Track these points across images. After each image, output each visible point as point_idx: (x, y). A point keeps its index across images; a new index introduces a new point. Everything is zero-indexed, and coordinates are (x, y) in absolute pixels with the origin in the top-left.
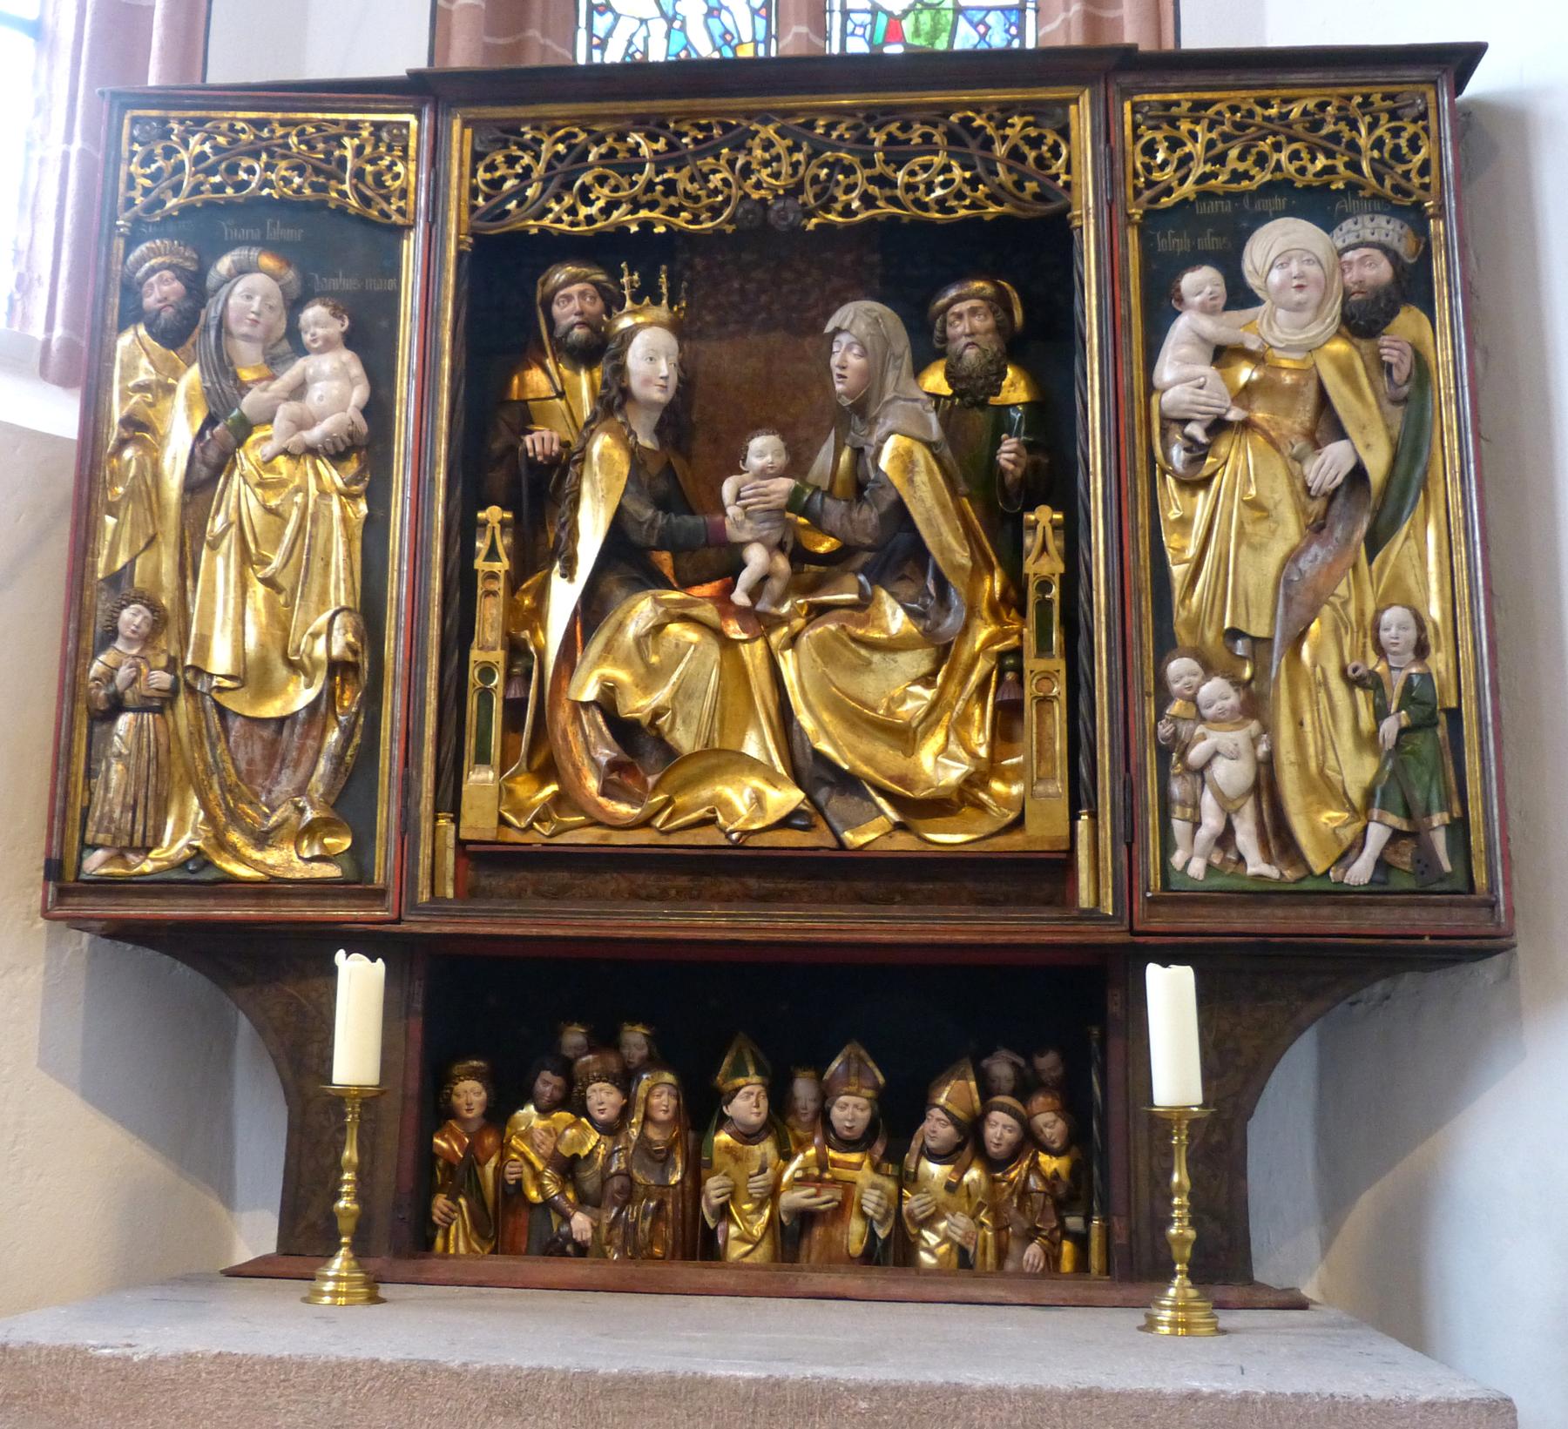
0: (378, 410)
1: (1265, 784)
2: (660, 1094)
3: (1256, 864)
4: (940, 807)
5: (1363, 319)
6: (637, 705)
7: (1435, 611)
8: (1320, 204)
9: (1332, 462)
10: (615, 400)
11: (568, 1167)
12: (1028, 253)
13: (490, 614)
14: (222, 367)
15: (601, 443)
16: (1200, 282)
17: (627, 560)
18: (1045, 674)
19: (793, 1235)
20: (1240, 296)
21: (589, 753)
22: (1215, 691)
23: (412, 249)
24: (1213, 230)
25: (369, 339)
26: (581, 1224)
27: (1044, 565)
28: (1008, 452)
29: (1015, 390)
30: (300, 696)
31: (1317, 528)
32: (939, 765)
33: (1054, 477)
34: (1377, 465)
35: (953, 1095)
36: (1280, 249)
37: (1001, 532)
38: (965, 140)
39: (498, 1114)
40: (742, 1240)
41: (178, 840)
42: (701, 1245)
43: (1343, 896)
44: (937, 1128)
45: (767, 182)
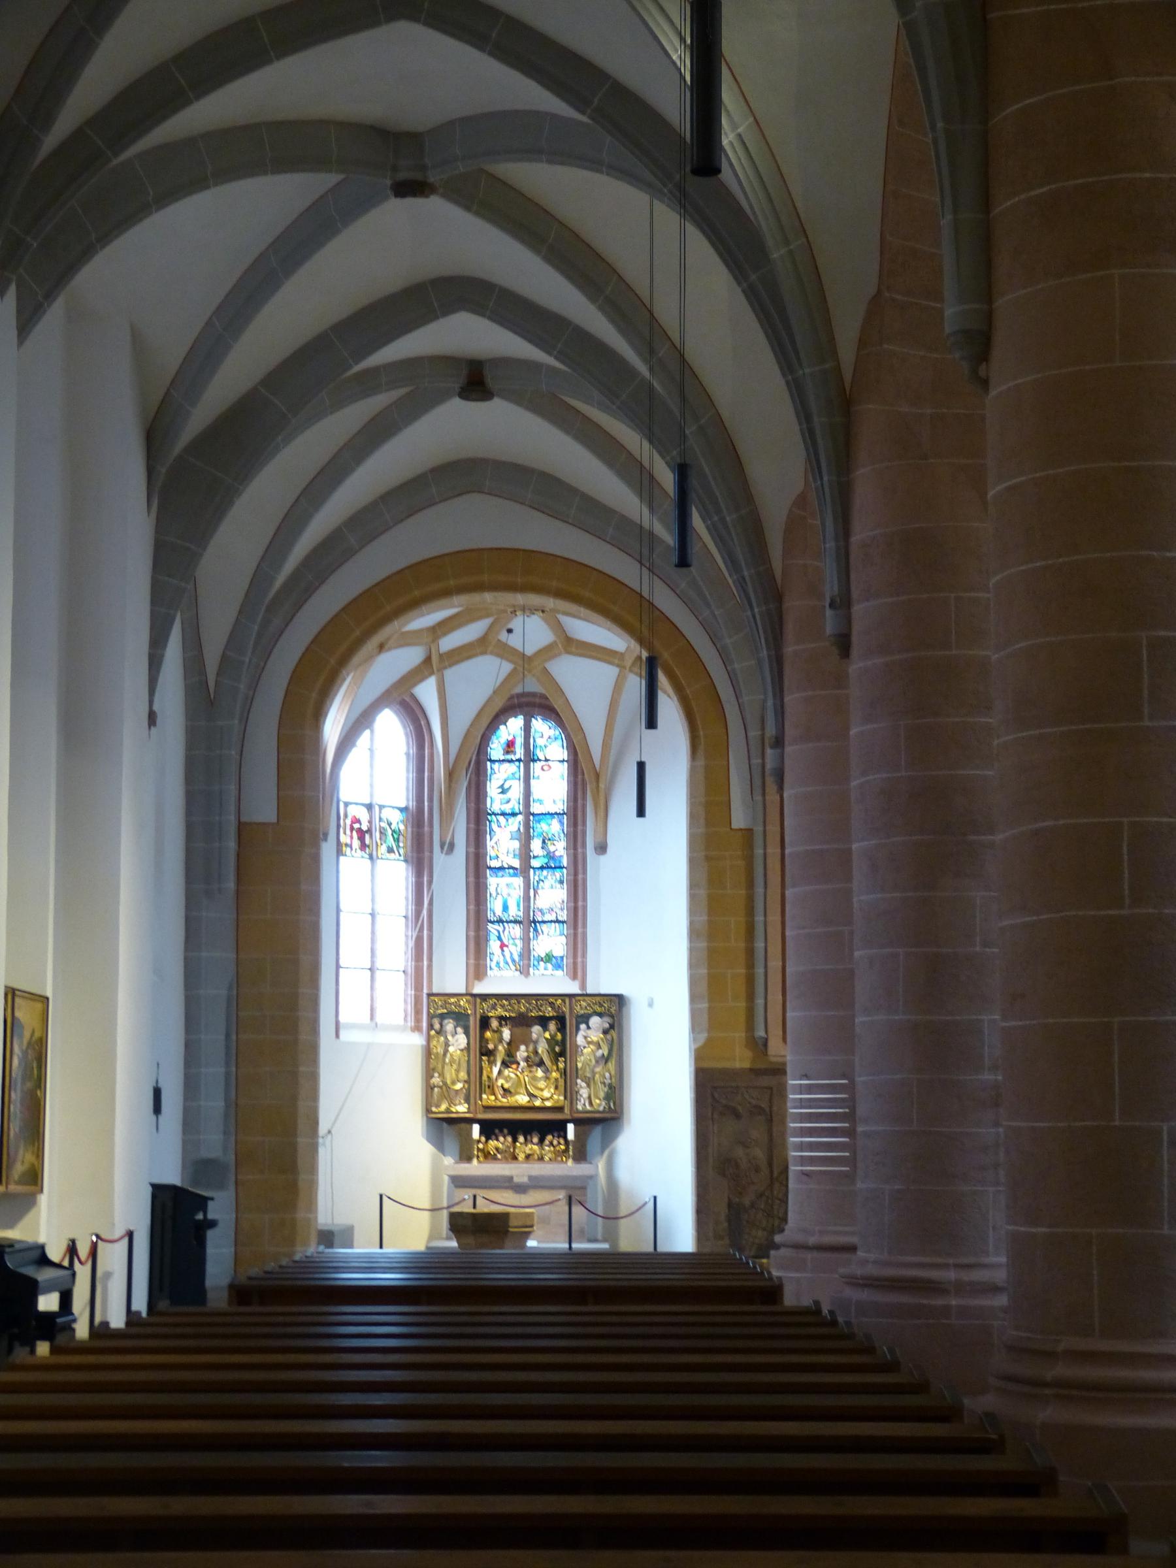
0: (468, 1044)
1: (589, 1098)
2: (509, 1139)
3: (588, 1108)
4: (547, 1099)
5: (605, 1032)
6: (506, 1086)
7: (613, 1073)
8: (600, 1015)
9: (600, 1053)
10: (501, 1040)
11: (497, 1149)
12: (561, 1020)
13: (485, 1073)
14: (446, 1038)
15: (500, 1048)
16: (583, 1026)
17: (505, 1064)
18: (561, 1082)
19: (528, 1157)
20: (589, 1028)
21: (499, 1092)
22: (584, 1084)
23: (472, 1019)
24: (585, 1019)
25: (467, 1033)
26: (499, 1156)
27: (561, 1065)
28: (557, 1049)
29: (559, 1036)
30: (459, 1086)
31: (597, 1062)
32: (546, 1094)
33: (562, 1054)
34: (606, 1054)
35: (549, 1137)
36: (595, 1021)
37: (555, 1061)
38: (552, 1004)
39: (487, 1141)
40: (521, 1157)
41: (443, 1107)
42: (515, 1158)
43: (599, 1112)
44: (547, 1142)
45: (523, 1009)
